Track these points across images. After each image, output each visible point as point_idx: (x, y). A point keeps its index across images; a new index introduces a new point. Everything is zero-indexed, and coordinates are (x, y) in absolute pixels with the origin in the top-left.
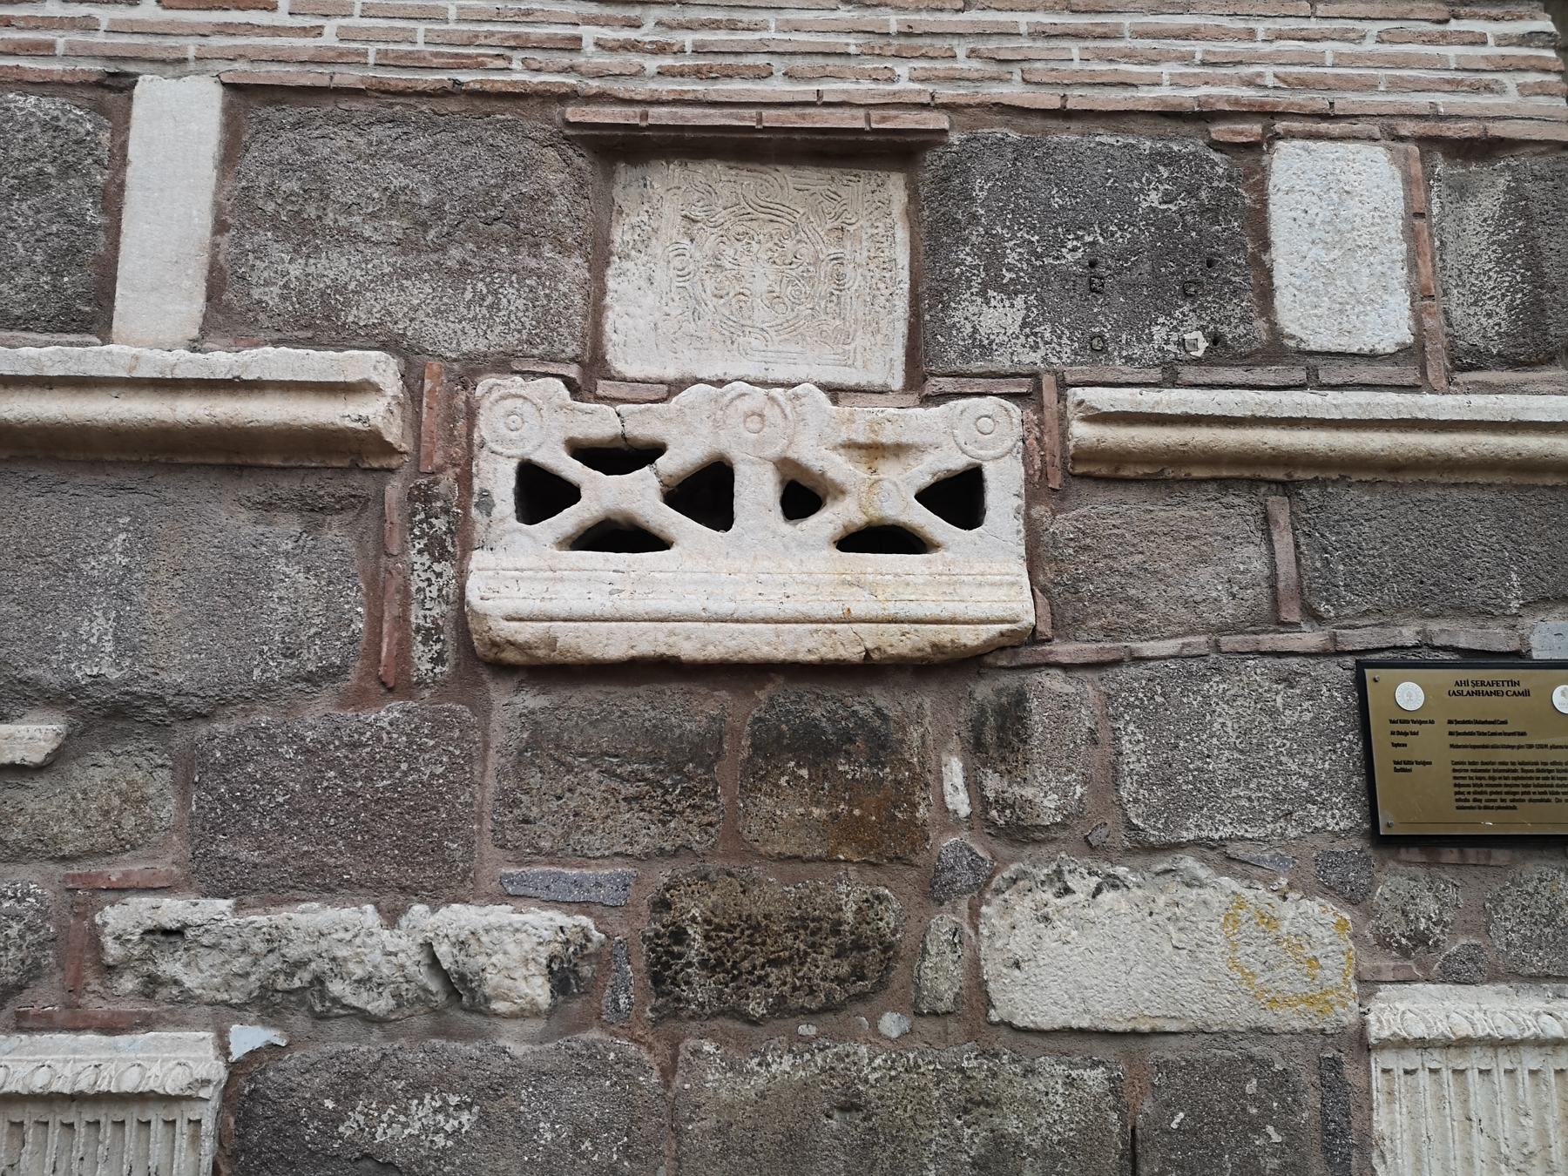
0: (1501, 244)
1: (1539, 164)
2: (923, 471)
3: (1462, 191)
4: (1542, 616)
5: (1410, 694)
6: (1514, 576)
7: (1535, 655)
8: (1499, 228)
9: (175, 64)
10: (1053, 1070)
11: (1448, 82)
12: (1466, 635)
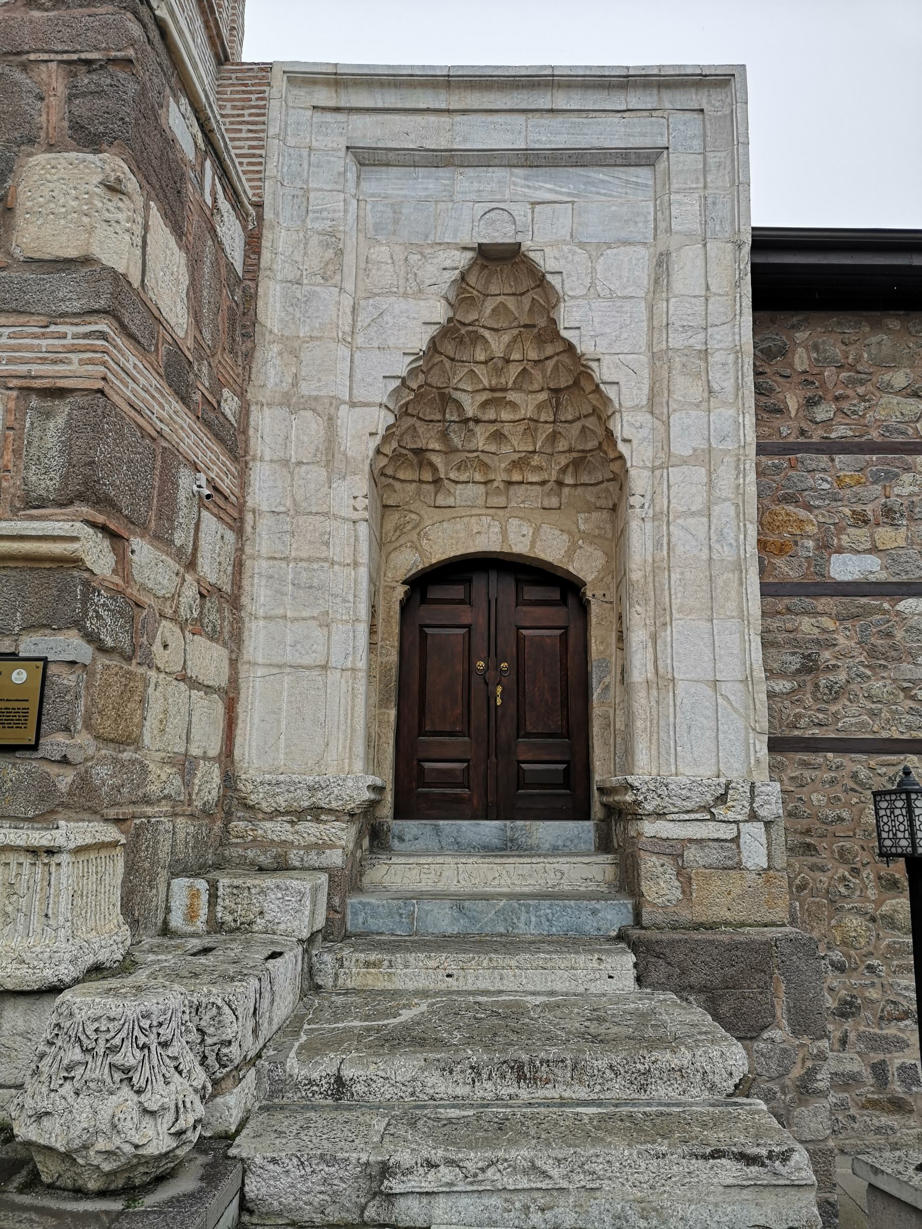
0: (62, 442)
1: (81, 400)
3: (48, 415)
4: (31, 634)
6: (18, 614)
7: (21, 655)
8: (63, 434)
11: (40, 358)
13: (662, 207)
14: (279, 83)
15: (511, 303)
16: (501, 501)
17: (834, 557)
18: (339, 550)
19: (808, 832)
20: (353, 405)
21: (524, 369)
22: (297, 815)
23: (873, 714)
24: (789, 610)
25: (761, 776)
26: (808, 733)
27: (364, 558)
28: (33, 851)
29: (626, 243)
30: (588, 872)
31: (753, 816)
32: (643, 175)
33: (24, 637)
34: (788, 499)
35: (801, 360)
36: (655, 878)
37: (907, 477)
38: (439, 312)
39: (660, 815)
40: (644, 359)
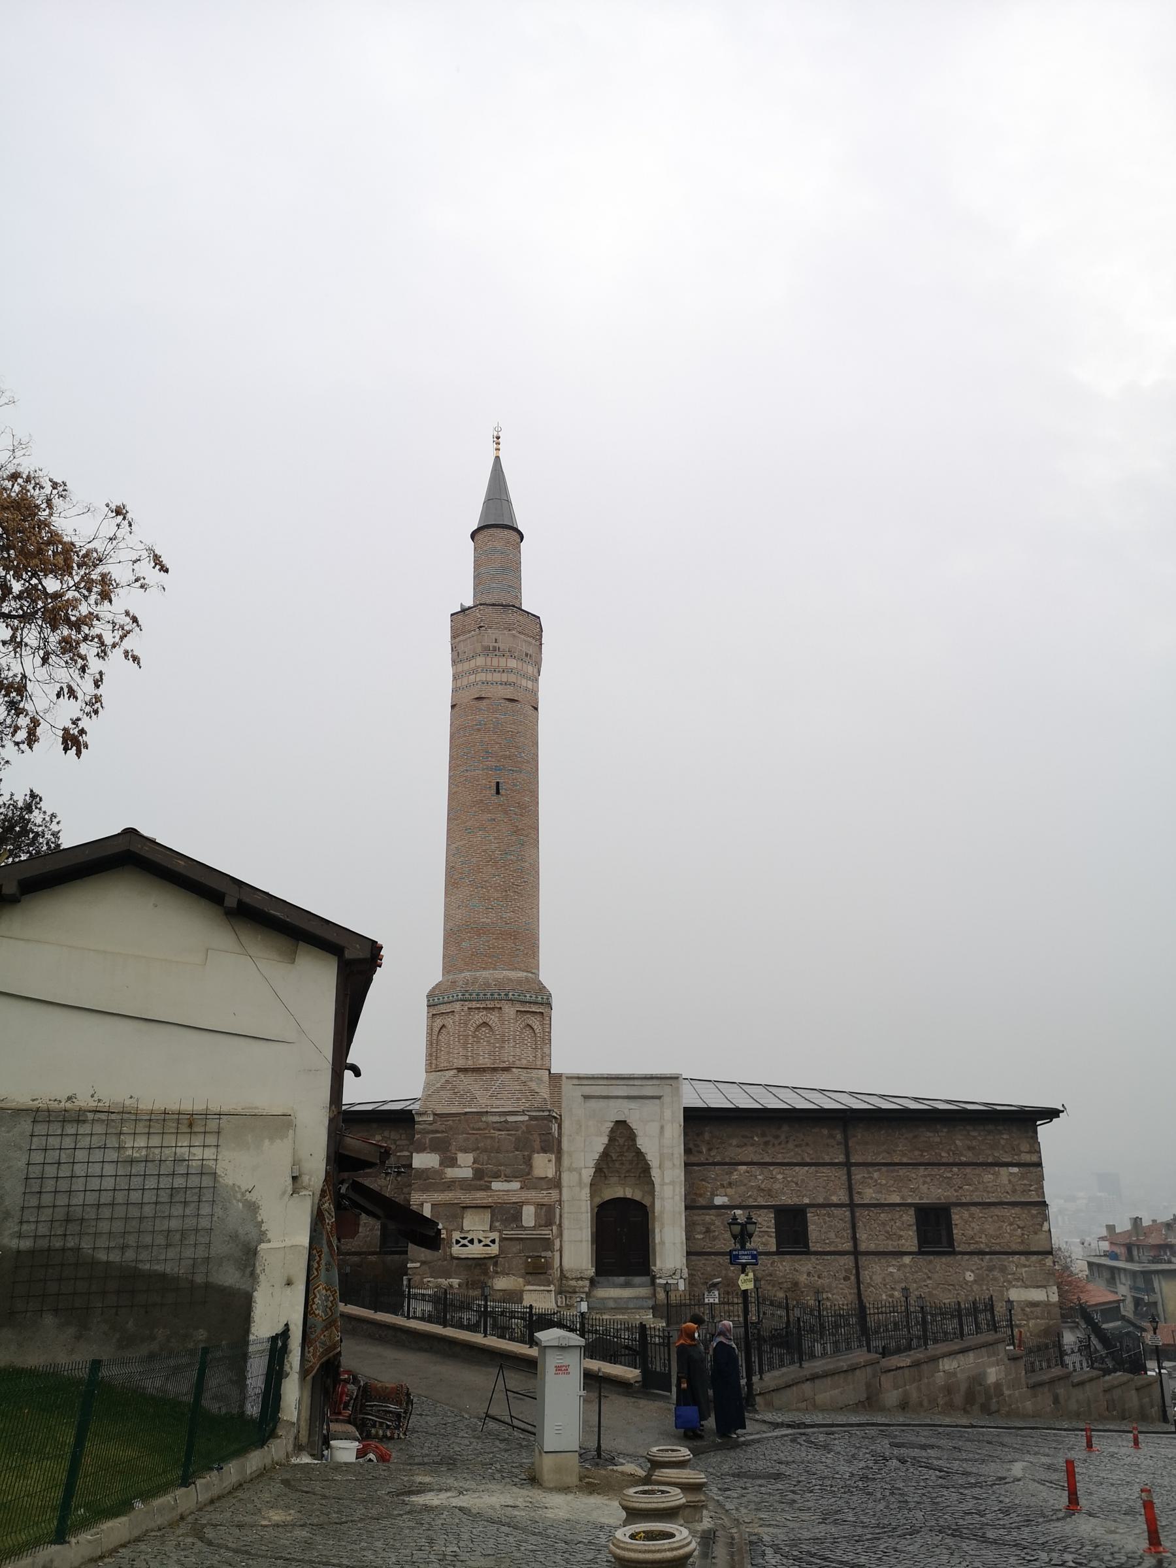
2: (490, 1239)
3: (541, 1209)
5: (529, 1260)
9: (427, 1202)
10: (498, 1293)
12: (536, 1254)
13: (662, 1113)
14: (564, 1078)
15: (625, 1131)
16: (623, 1182)
17: (716, 1198)
18: (584, 1209)
19: (706, 1279)
20: (585, 1168)
21: (629, 1148)
22: (577, 1279)
23: (725, 1244)
24: (703, 1214)
25: (684, 1267)
26: (709, 1250)
27: (589, 1211)
28: (548, 1291)
29: (653, 1121)
30: (646, 1291)
31: (681, 1278)
32: (658, 1100)
33: (566, 1265)
34: (702, 1180)
35: (707, 1136)
36: (659, 1293)
37: (735, 1173)
38: (605, 1140)
39: (660, 1278)
40: (658, 1154)
